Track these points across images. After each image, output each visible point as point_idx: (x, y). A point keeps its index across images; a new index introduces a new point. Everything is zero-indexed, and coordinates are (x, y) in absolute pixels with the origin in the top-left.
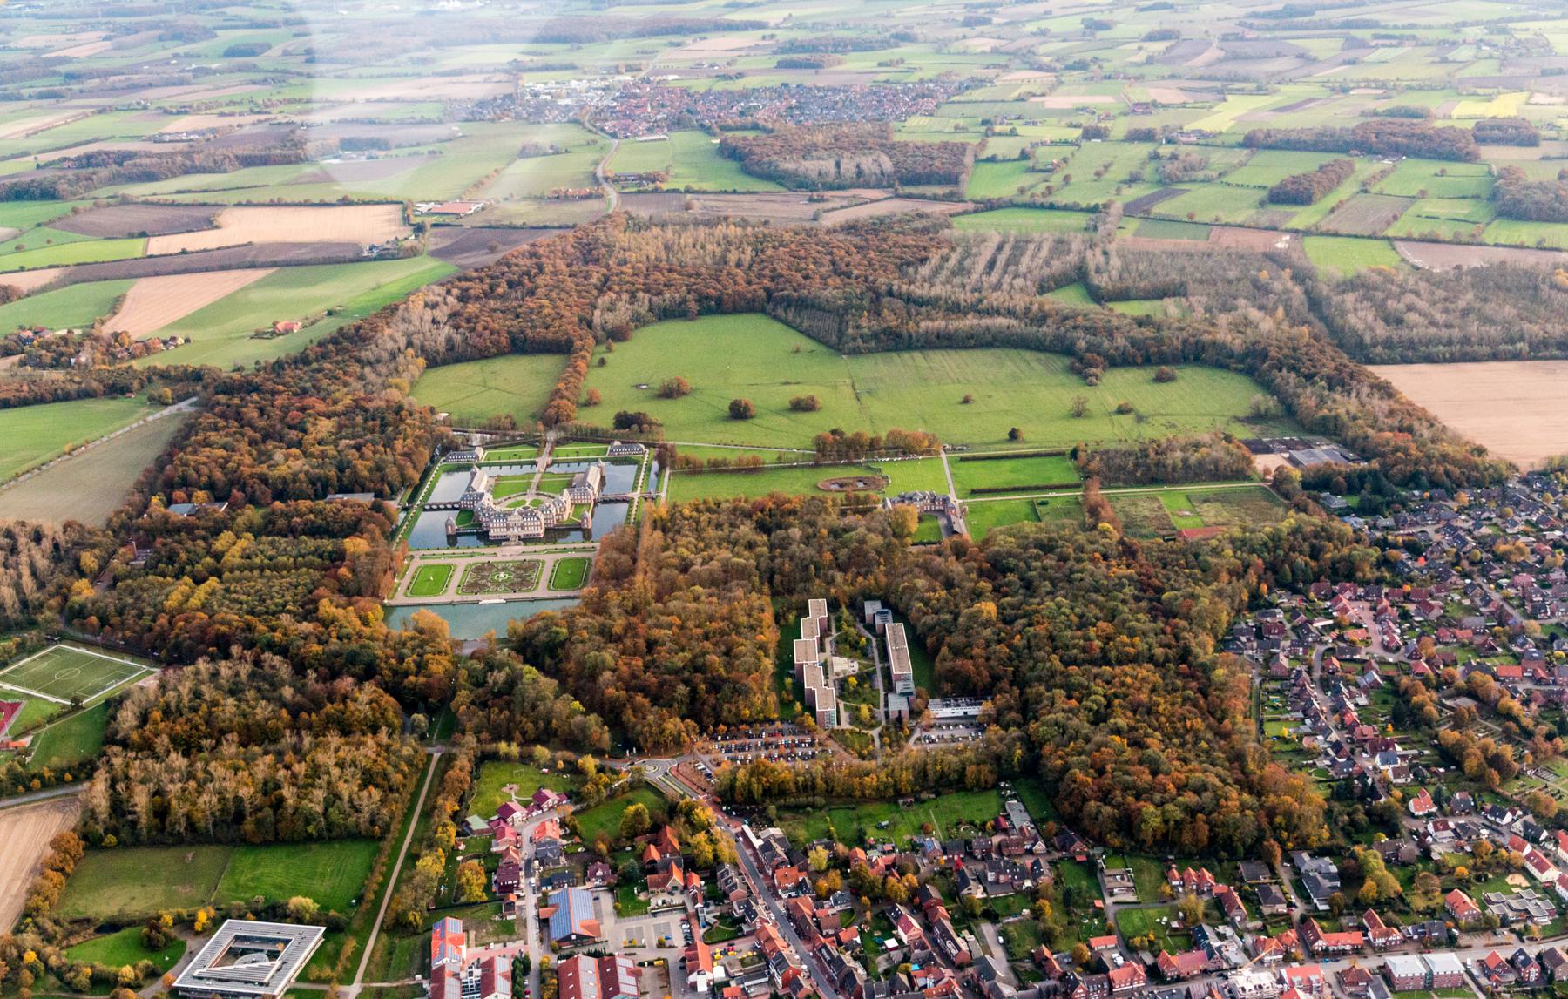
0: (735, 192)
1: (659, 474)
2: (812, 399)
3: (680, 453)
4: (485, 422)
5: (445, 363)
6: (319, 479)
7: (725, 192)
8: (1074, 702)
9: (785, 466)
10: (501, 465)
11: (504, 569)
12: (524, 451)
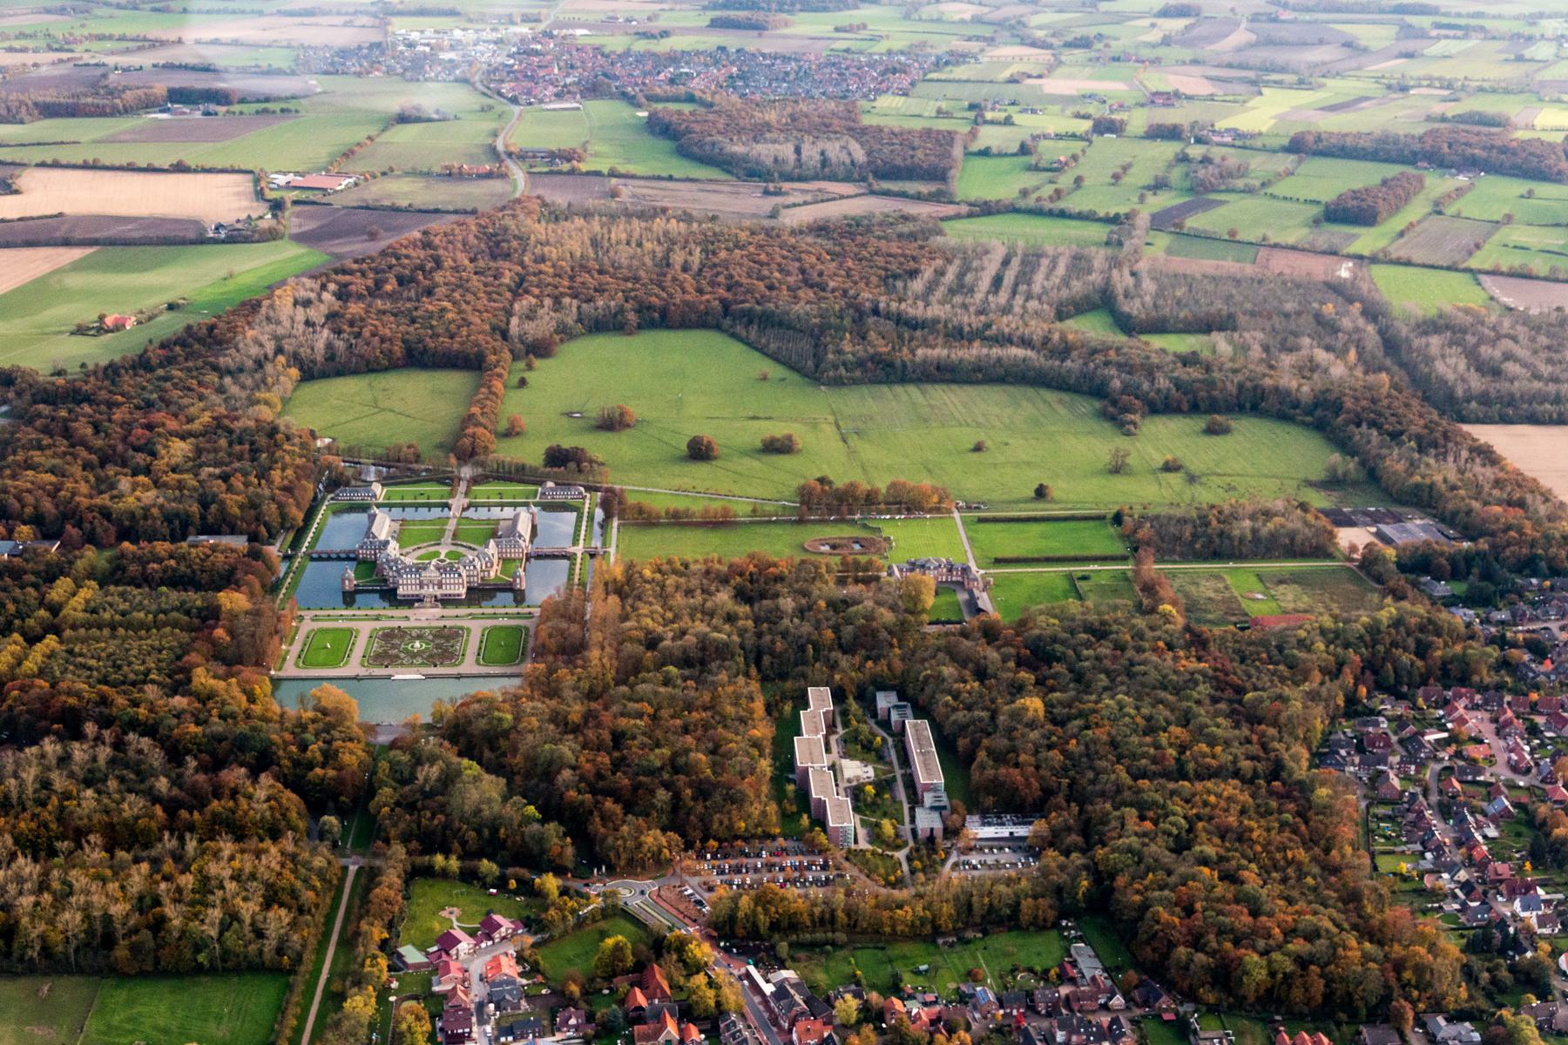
0: (670, 178)
1: (604, 526)
2: (789, 438)
3: (631, 500)
4: (379, 451)
5: (325, 375)
6: (177, 515)
7: (659, 178)
8: (1148, 825)
9: (760, 520)
10: (404, 506)
11: (419, 637)
12: (433, 490)
